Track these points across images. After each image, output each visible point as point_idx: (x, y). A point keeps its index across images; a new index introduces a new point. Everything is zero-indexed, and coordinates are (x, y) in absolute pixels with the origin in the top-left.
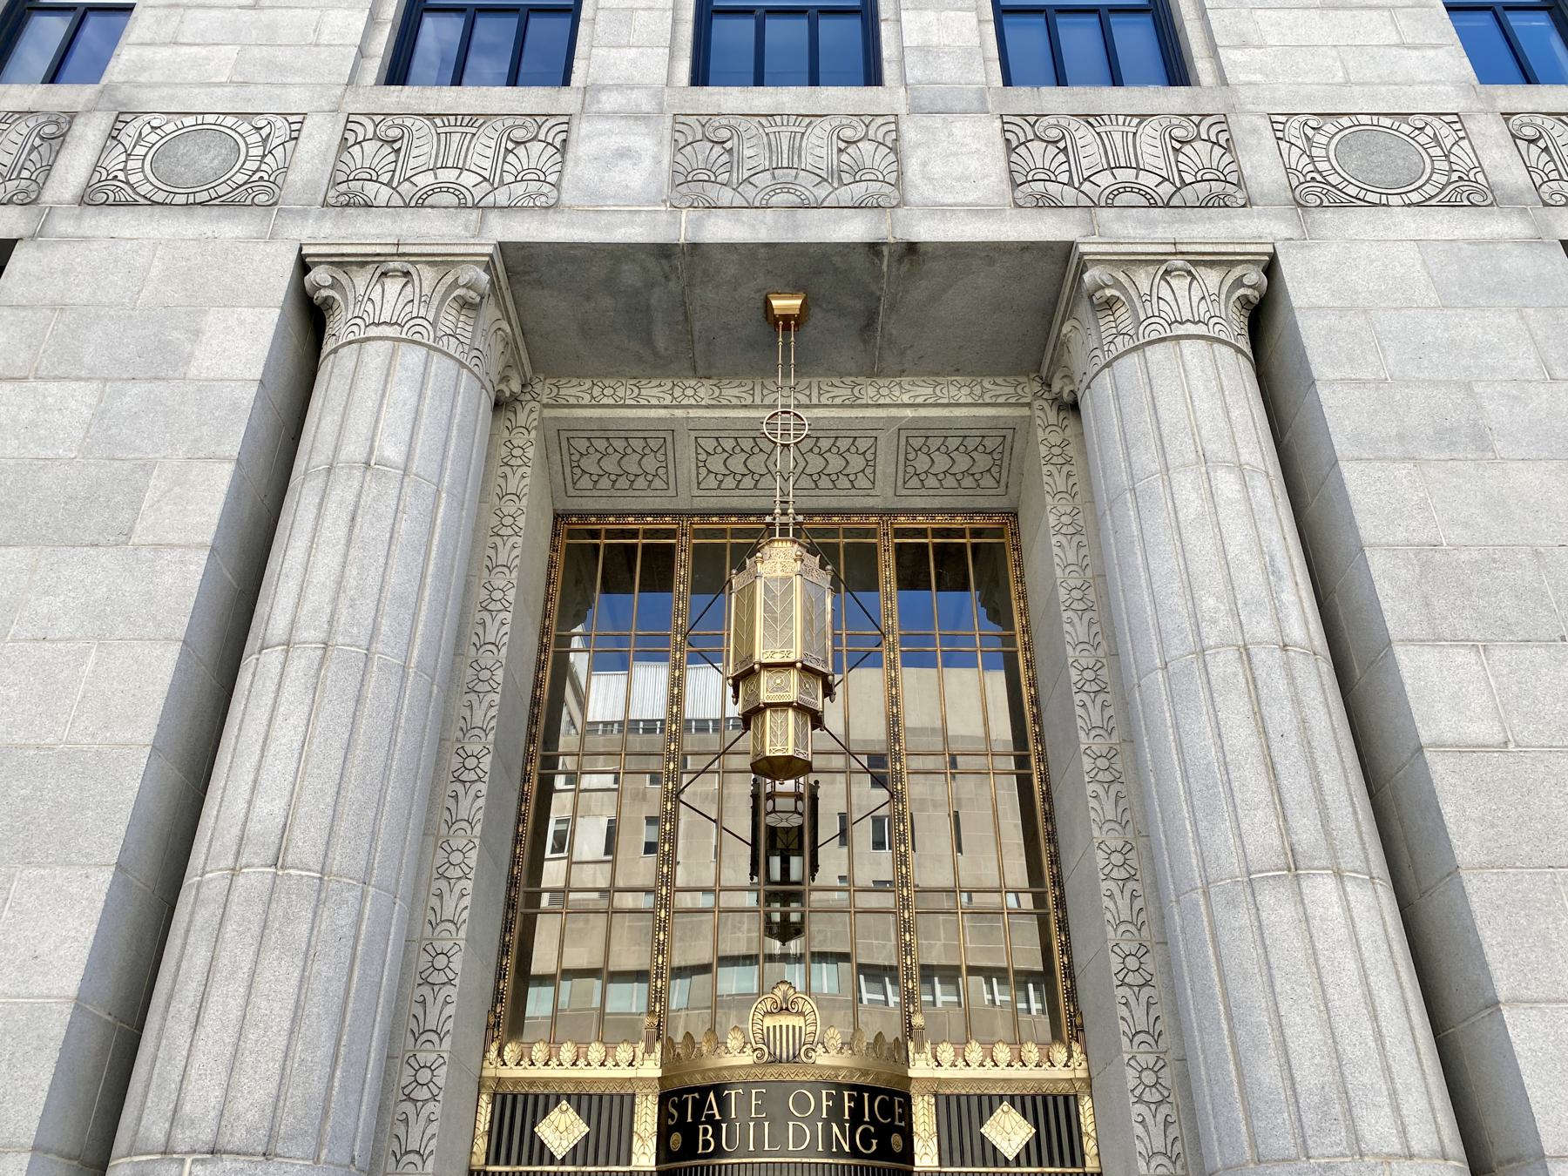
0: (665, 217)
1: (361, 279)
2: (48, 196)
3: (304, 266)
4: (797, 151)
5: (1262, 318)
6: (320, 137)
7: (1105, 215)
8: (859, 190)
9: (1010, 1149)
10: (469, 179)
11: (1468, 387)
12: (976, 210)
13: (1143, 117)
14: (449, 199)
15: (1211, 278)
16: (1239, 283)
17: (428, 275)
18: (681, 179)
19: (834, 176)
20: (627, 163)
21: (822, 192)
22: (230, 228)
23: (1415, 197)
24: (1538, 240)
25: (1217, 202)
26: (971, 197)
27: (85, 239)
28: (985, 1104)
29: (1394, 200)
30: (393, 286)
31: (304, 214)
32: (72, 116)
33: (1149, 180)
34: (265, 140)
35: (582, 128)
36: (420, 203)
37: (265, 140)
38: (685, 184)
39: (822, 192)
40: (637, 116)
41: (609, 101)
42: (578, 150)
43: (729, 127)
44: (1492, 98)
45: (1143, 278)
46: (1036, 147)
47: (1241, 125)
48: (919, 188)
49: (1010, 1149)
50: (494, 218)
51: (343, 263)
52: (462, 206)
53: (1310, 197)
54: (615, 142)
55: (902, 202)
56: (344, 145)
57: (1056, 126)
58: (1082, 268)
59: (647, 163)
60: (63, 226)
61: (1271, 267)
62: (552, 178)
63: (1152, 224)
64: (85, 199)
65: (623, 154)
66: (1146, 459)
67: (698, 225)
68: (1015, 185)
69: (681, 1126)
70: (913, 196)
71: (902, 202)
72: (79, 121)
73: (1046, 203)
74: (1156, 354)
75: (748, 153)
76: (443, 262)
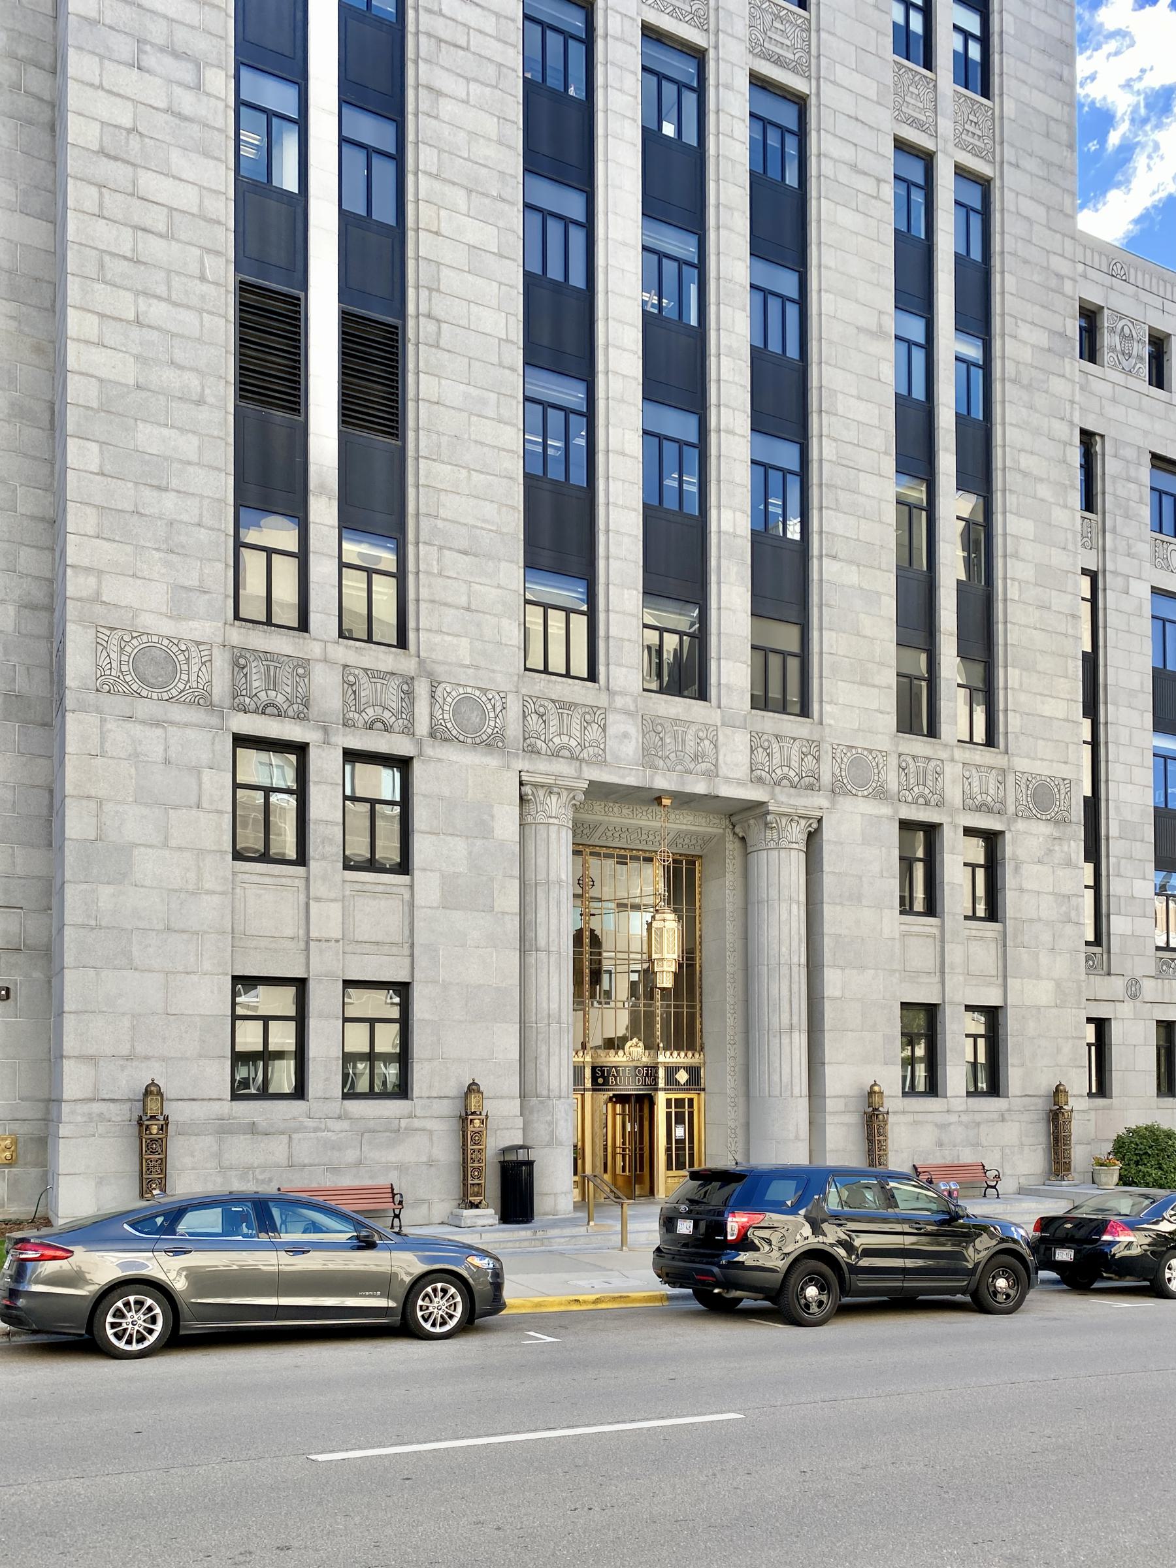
0: (641, 773)
1: (541, 793)
2: (417, 732)
3: (521, 784)
4: (683, 741)
5: (813, 838)
6: (514, 708)
7: (777, 789)
8: (703, 766)
9: (682, 1081)
10: (573, 743)
11: (860, 878)
12: (740, 783)
13: (795, 739)
14: (567, 753)
15: (803, 822)
16: (810, 825)
17: (565, 793)
18: (646, 752)
19: (698, 757)
20: (626, 741)
21: (692, 766)
22: (493, 761)
23: (866, 793)
24: (891, 818)
25: (810, 787)
26: (737, 776)
27: (439, 760)
28: (677, 1069)
29: (860, 794)
30: (554, 798)
31: (517, 755)
32: (412, 678)
33: (792, 774)
34: (494, 707)
35: (611, 718)
36: (556, 754)
37: (494, 707)
38: (649, 757)
39: (692, 766)
40: (629, 714)
41: (619, 702)
42: (611, 731)
43: (661, 725)
44: (897, 745)
45: (784, 821)
46: (760, 750)
47: (826, 747)
48: (723, 770)
49: (682, 1081)
50: (585, 767)
51: (535, 786)
52: (572, 758)
53: (837, 790)
54: (622, 728)
55: (717, 776)
56: (524, 717)
57: (767, 740)
58: (768, 813)
59: (634, 741)
60: (429, 751)
61: (820, 821)
62: (602, 746)
63: (789, 796)
64: (432, 735)
65: (626, 735)
66: (774, 893)
67: (652, 778)
68: (752, 771)
69: (603, 1076)
70: (720, 774)
71: (717, 776)
72: (416, 683)
73: (760, 780)
74: (783, 853)
75: (668, 741)
76: (570, 789)
